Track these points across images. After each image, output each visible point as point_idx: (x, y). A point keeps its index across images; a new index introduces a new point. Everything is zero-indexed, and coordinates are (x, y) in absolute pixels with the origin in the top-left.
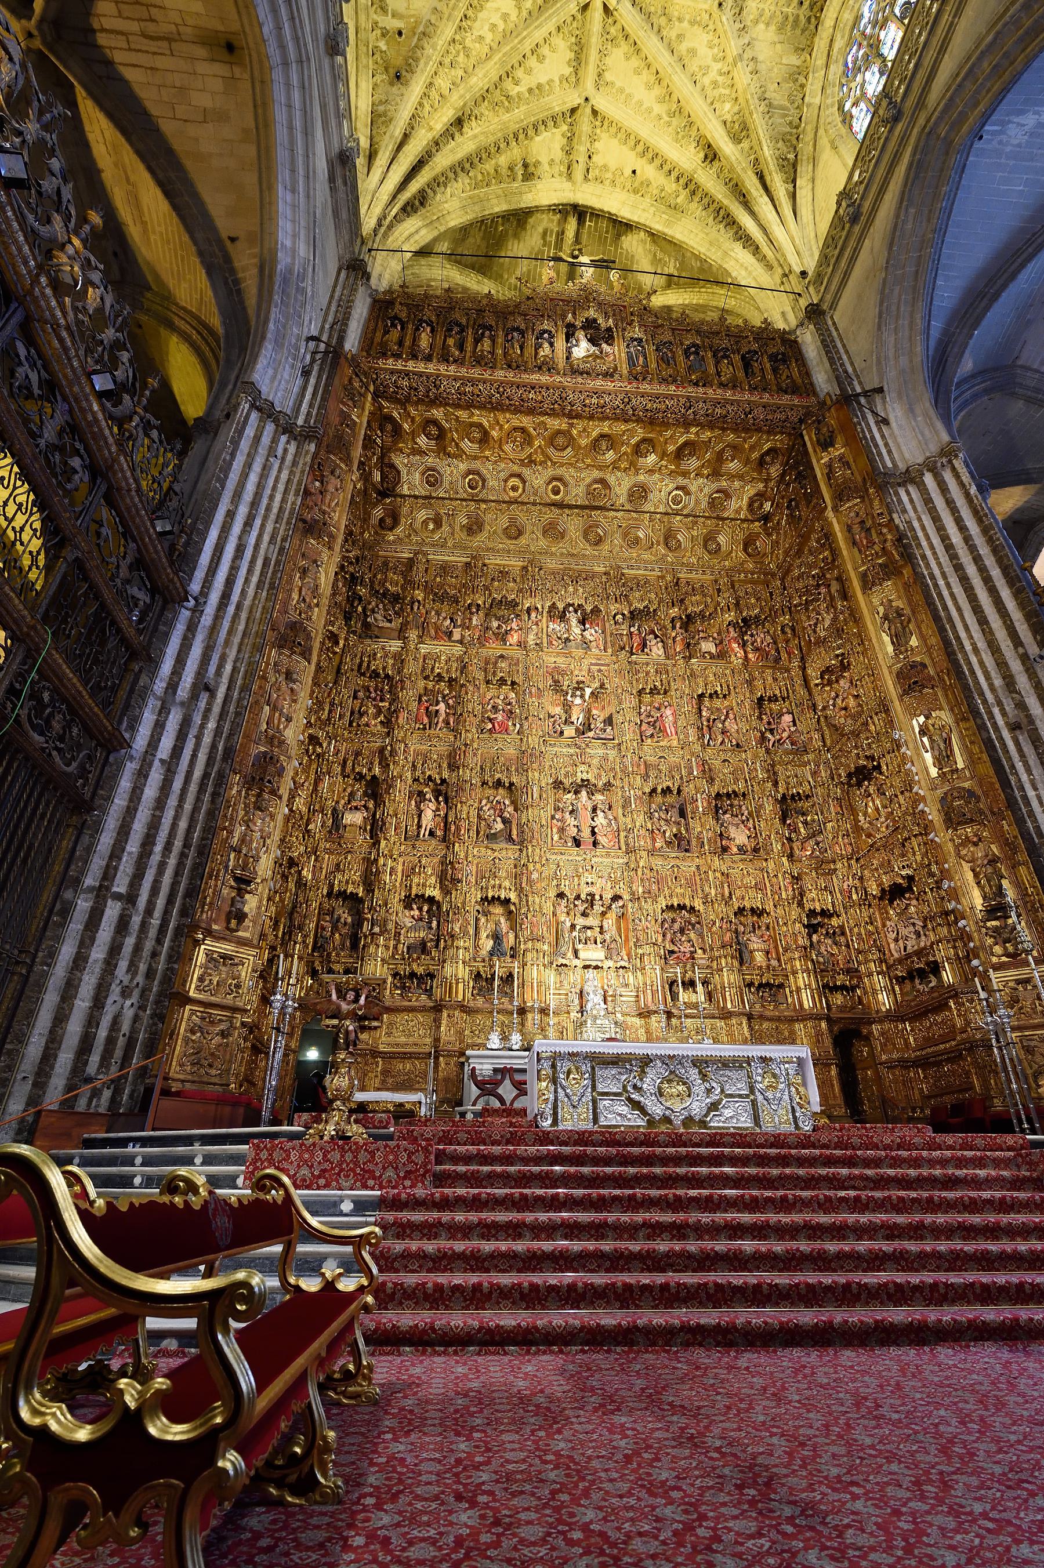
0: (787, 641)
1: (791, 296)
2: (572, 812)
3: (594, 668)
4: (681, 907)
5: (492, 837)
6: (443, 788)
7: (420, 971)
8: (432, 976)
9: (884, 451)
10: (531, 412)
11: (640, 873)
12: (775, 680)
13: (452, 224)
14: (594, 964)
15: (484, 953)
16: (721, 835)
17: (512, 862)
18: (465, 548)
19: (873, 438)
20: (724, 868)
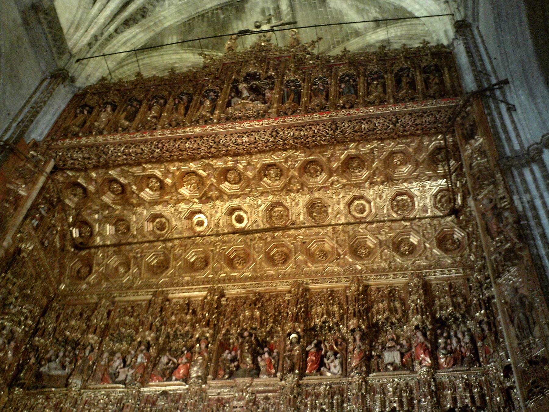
0: (483, 338)
1: (451, 16)
3: (260, 396)
9: (513, 135)
10: (193, 159)
12: (468, 386)
13: (168, 24)
18: (151, 287)
19: (504, 125)
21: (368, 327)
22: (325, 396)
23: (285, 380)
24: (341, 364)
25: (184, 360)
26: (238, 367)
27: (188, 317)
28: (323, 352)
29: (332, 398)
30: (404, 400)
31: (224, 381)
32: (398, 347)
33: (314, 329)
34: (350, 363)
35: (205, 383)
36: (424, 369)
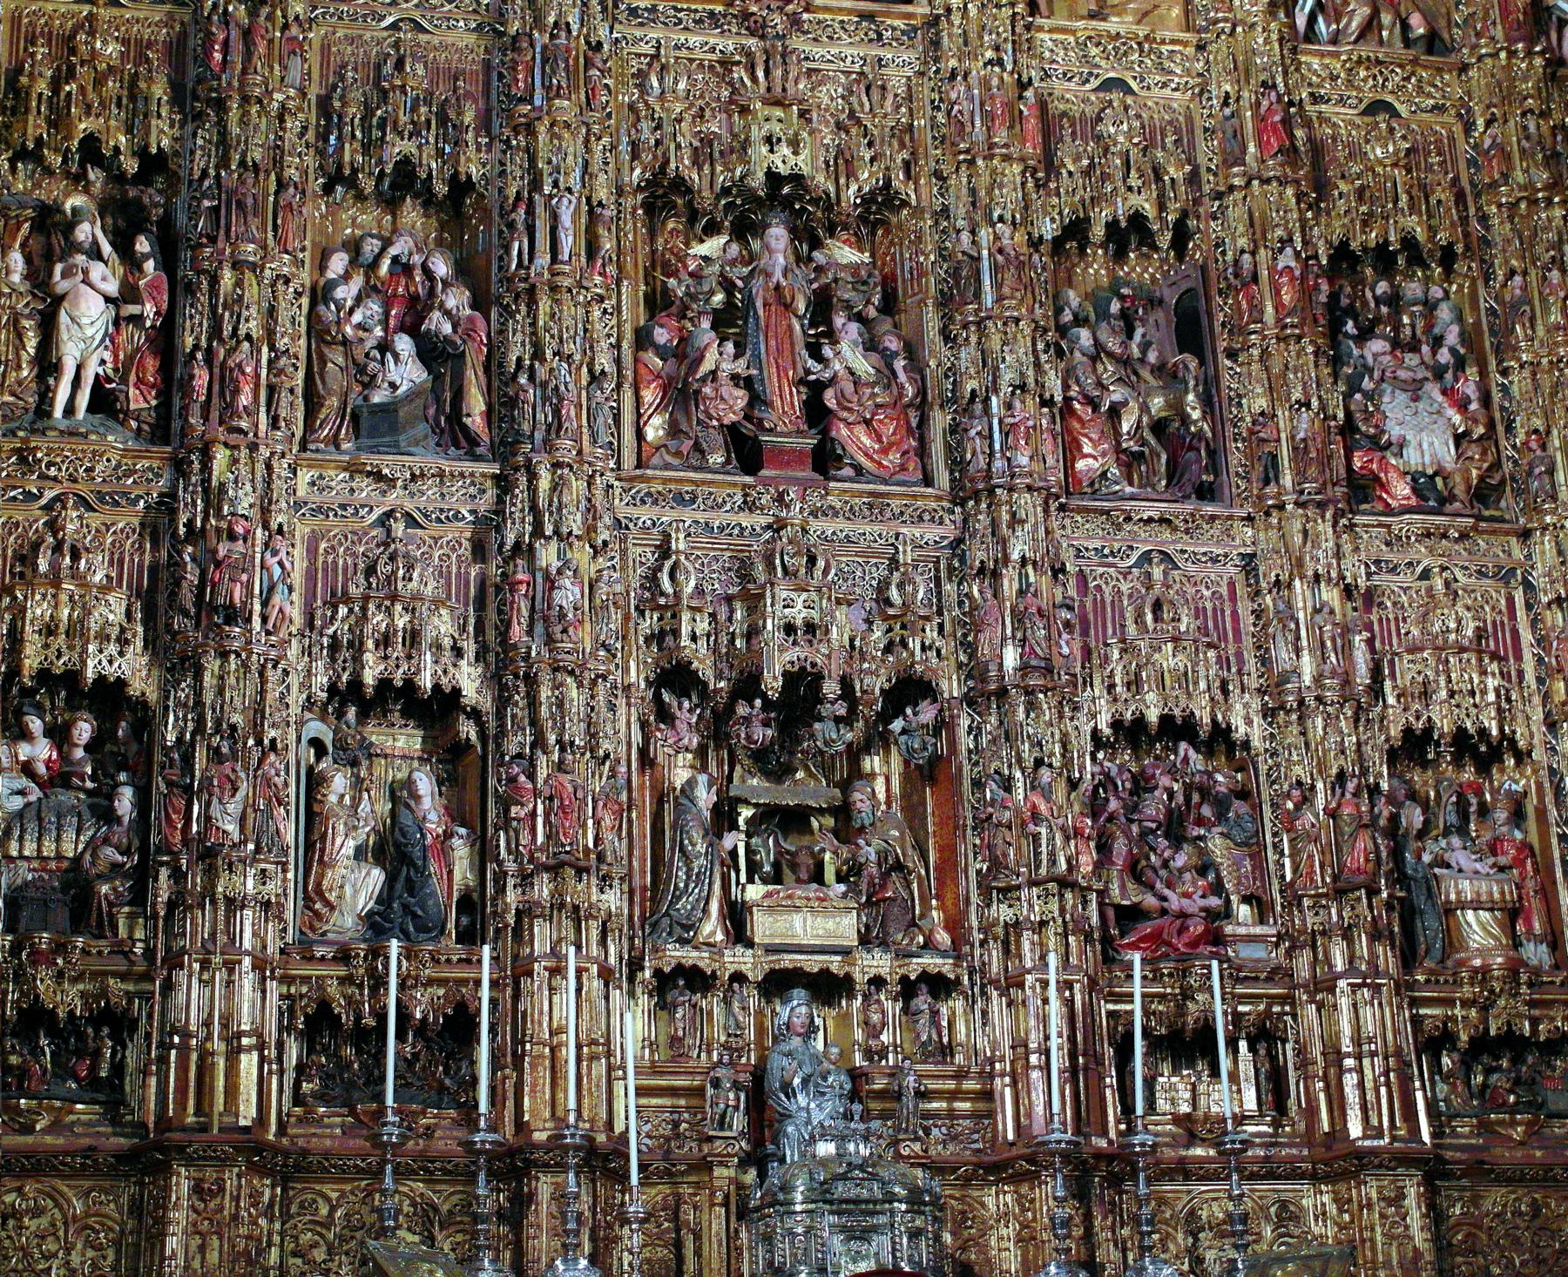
2: (723, 321)
4: (1177, 729)
6: (152, 197)
7: (68, 999)
8: (119, 1024)
11: (1009, 585)
14: (812, 964)
15: (346, 922)
16: (1348, 428)
17: (462, 532)
20: (1354, 570)
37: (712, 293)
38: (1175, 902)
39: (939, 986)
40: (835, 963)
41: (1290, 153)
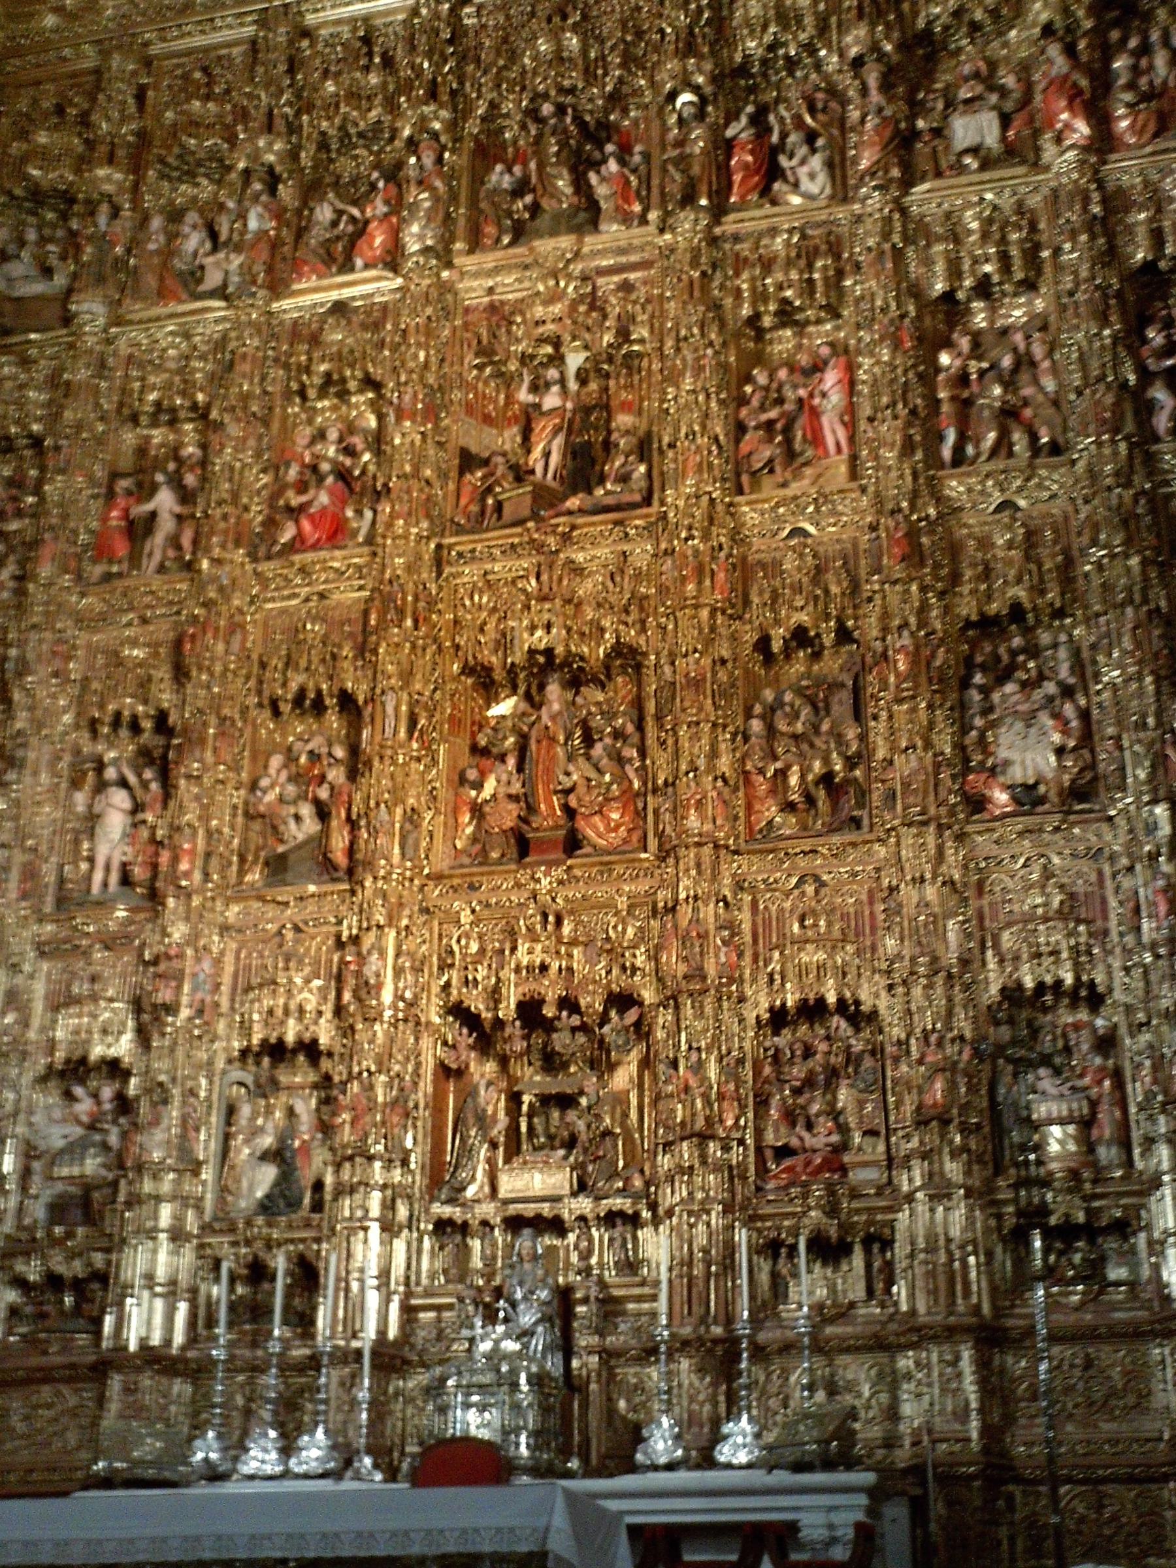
4: (813, 1010)
5: (278, 867)
14: (529, 1210)
21: (901, 47)
22: (789, 263)
23: (673, 230)
24: (830, 165)
25: (381, 209)
26: (535, 209)
27: (374, 79)
28: (775, 138)
29: (810, 266)
30: (1014, 252)
31: (499, 254)
32: (994, 98)
33: (743, 70)
34: (855, 161)
35: (449, 265)
36: (1071, 155)
37: (505, 738)
38: (809, 1140)
39: (634, 1221)
40: (546, 1209)
41: (914, 556)
